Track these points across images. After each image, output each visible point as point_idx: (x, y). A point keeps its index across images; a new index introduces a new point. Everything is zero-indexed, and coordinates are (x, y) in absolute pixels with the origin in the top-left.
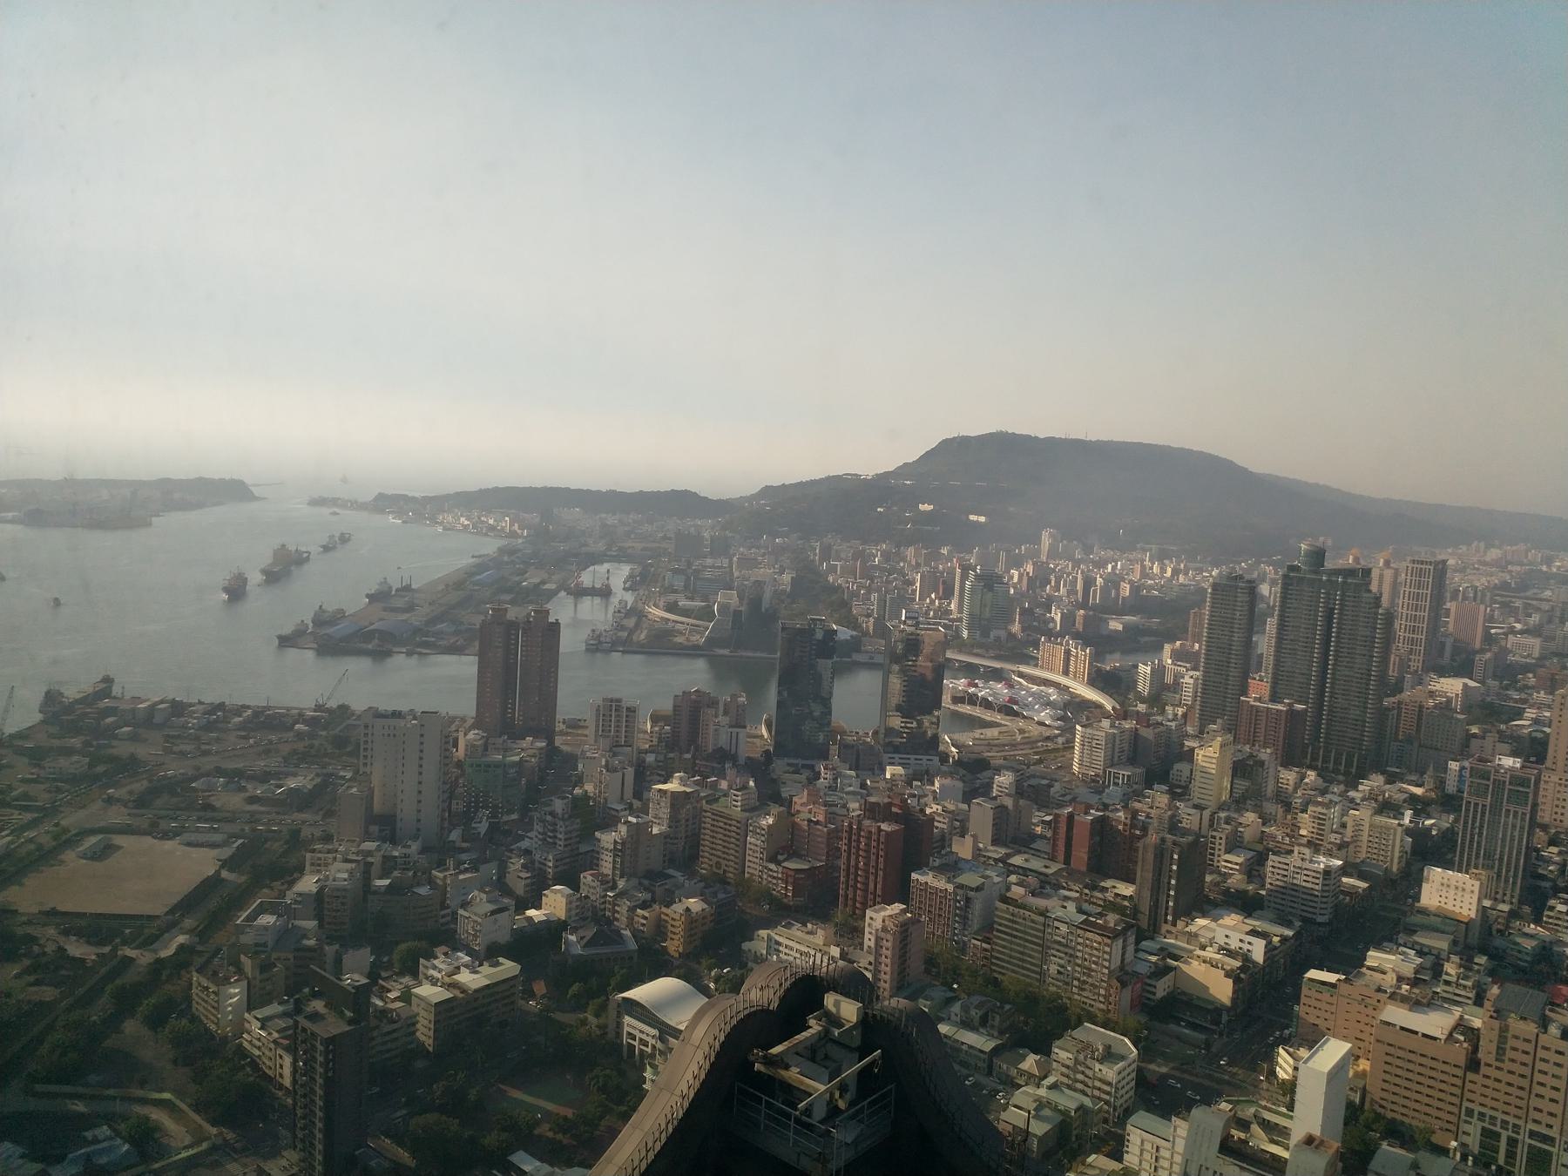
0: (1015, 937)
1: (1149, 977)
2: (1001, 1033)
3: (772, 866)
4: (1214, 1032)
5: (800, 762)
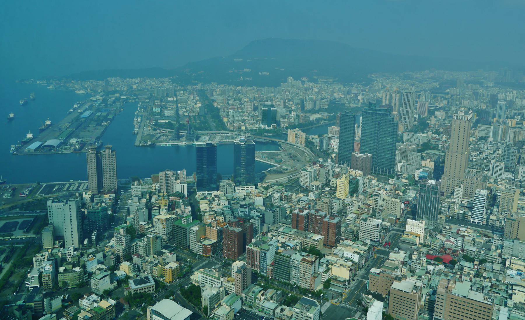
0: (281, 265)
1: (323, 273)
2: (277, 302)
3: (199, 244)
4: (344, 288)
5: (206, 192)
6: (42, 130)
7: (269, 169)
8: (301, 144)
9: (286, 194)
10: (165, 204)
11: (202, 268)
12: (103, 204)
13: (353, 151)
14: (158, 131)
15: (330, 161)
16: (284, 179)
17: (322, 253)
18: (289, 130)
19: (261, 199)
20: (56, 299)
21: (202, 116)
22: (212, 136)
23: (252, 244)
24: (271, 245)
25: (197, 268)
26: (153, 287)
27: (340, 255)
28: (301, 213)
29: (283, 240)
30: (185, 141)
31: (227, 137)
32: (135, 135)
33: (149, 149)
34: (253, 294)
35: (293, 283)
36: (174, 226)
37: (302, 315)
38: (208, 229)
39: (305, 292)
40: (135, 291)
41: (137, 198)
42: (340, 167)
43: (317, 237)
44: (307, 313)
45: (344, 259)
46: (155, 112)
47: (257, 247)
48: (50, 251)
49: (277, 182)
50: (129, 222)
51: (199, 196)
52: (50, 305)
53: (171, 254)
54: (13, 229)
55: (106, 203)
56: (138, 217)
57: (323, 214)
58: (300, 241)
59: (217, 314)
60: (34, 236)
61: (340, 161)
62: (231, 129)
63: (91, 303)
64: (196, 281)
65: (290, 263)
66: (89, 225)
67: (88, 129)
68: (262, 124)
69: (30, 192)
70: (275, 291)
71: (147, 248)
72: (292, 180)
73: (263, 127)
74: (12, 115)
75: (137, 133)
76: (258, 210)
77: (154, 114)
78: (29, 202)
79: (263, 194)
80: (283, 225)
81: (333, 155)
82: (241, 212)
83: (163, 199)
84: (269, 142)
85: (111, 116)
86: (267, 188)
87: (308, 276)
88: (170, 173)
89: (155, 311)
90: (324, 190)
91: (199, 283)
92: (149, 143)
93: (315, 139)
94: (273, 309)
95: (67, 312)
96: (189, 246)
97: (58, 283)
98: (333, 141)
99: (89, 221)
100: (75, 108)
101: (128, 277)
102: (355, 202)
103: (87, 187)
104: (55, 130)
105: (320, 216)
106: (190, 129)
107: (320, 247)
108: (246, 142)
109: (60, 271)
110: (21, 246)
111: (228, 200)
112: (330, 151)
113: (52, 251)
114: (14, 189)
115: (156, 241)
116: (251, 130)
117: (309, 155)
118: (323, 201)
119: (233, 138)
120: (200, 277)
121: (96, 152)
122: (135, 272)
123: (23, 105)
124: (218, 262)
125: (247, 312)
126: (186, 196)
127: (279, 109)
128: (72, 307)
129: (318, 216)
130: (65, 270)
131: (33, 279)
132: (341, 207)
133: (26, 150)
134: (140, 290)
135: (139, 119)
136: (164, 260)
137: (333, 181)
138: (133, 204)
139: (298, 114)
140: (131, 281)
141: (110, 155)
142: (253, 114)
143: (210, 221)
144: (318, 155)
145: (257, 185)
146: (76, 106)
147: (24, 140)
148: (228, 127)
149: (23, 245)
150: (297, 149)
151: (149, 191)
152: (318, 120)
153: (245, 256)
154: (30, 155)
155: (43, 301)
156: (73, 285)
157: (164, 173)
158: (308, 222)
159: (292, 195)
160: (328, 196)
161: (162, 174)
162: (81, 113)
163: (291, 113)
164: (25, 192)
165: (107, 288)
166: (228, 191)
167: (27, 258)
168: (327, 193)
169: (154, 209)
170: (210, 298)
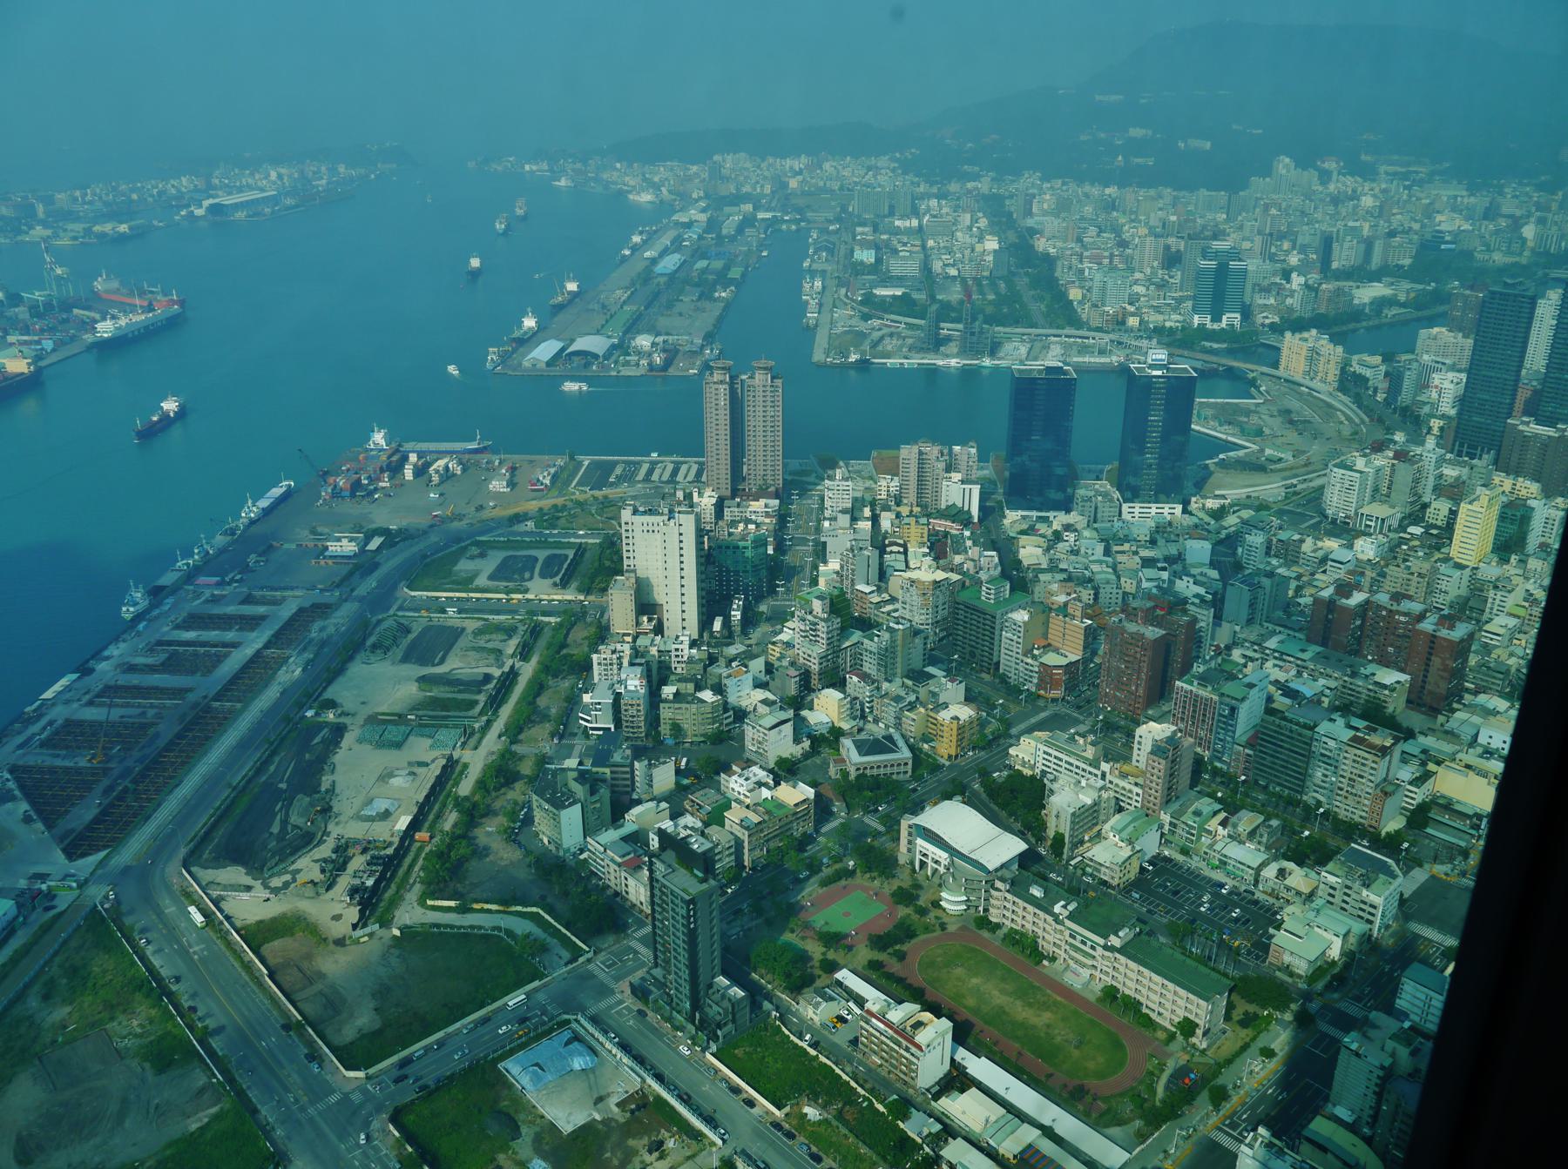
1: (1410, 783)
2: (1268, 848)
3: (1029, 661)
4: (1473, 836)
5: (1034, 514)
6: (560, 308)
7: (1221, 456)
8: (1323, 381)
9: (1283, 535)
10: (920, 540)
11: (1039, 726)
12: (752, 527)
13: (1509, 415)
14: (876, 323)
15: (1431, 442)
16: (1271, 489)
17: (1405, 725)
18: (1288, 334)
19: (1207, 546)
21: (999, 278)
22: (1038, 345)
23: (1194, 677)
24: (1251, 686)
25: (1022, 726)
26: (906, 764)
27: (1466, 737)
28: (1344, 601)
29: (1281, 676)
30: (957, 356)
31: (1083, 350)
32: (811, 331)
33: (852, 373)
34: (1197, 819)
35: (1312, 802)
36: (955, 605)
37: (1345, 894)
38: (1056, 622)
39: (1350, 831)
40: (858, 769)
41: (848, 517)
42: (1459, 464)
43: (1389, 677)
44: (1365, 893)
45: (1480, 750)
46: (862, 263)
47: (1210, 688)
48: (629, 639)
49: (1249, 497)
50: (827, 583)
51: (1015, 522)
53: (952, 681)
54: (527, 575)
55: (758, 525)
56: (853, 570)
57: (1416, 607)
58: (1333, 684)
59: (1091, 860)
60: (582, 598)
61: (1462, 445)
62: (1095, 323)
63: (751, 787)
64: (1024, 764)
65: (1310, 745)
66: (721, 581)
67: (679, 307)
68: (1195, 310)
69: (555, 478)
70: (1262, 818)
71: (886, 658)
72: (1295, 493)
73: (1196, 320)
74: (475, 263)
75: (816, 325)
76: (1199, 578)
77: (859, 269)
78: (555, 506)
79: (1209, 532)
80: (1278, 629)
81: (1436, 424)
82: (1149, 580)
83: (913, 523)
84: (1216, 370)
85: (735, 273)
86: (1219, 514)
87: (1366, 787)
88: (932, 451)
89: (924, 828)
90: (1405, 532)
91: (1033, 767)
92: (853, 358)
93: (1370, 366)
94: (1255, 865)
96: (998, 663)
97: (658, 724)
98: (1436, 379)
99: (720, 571)
100: (636, 244)
101: (836, 733)
102: (1516, 580)
103: (699, 474)
104: (591, 307)
105: (1405, 614)
106: (974, 319)
107: (1395, 705)
108: (1168, 369)
110: (552, 620)
111: (1102, 540)
112: (1426, 409)
114: (513, 469)
115: (913, 642)
116: (1159, 331)
117: (1348, 418)
118: (1408, 568)
119: (1102, 352)
120: (1040, 753)
121: (731, 377)
122: (854, 719)
123: (505, 233)
124: (1082, 718)
125: (1176, 865)
126: (976, 520)
127: (1253, 265)
129: (1398, 612)
130: (677, 694)
132: (1464, 592)
133: (526, 364)
134: (872, 768)
135: (818, 284)
136: (934, 695)
137: (1439, 509)
138: (840, 537)
139: (1310, 282)
140: (847, 743)
141: (769, 388)
142: (1162, 279)
143: (1062, 599)
144: (1380, 421)
145: (1189, 502)
146: (636, 239)
147: (516, 334)
148: (1084, 317)
150: (1310, 399)
151: (868, 497)
152: (1380, 304)
153: (1165, 708)
155: (632, 766)
157: (915, 449)
158: (1361, 627)
159: (1302, 541)
160: (1421, 554)
161: (908, 453)
162: (654, 261)
163: (1288, 281)
165: (786, 755)
166: (1099, 515)
168: (1417, 543)
169: (891, 552)
170: (1073, 814)
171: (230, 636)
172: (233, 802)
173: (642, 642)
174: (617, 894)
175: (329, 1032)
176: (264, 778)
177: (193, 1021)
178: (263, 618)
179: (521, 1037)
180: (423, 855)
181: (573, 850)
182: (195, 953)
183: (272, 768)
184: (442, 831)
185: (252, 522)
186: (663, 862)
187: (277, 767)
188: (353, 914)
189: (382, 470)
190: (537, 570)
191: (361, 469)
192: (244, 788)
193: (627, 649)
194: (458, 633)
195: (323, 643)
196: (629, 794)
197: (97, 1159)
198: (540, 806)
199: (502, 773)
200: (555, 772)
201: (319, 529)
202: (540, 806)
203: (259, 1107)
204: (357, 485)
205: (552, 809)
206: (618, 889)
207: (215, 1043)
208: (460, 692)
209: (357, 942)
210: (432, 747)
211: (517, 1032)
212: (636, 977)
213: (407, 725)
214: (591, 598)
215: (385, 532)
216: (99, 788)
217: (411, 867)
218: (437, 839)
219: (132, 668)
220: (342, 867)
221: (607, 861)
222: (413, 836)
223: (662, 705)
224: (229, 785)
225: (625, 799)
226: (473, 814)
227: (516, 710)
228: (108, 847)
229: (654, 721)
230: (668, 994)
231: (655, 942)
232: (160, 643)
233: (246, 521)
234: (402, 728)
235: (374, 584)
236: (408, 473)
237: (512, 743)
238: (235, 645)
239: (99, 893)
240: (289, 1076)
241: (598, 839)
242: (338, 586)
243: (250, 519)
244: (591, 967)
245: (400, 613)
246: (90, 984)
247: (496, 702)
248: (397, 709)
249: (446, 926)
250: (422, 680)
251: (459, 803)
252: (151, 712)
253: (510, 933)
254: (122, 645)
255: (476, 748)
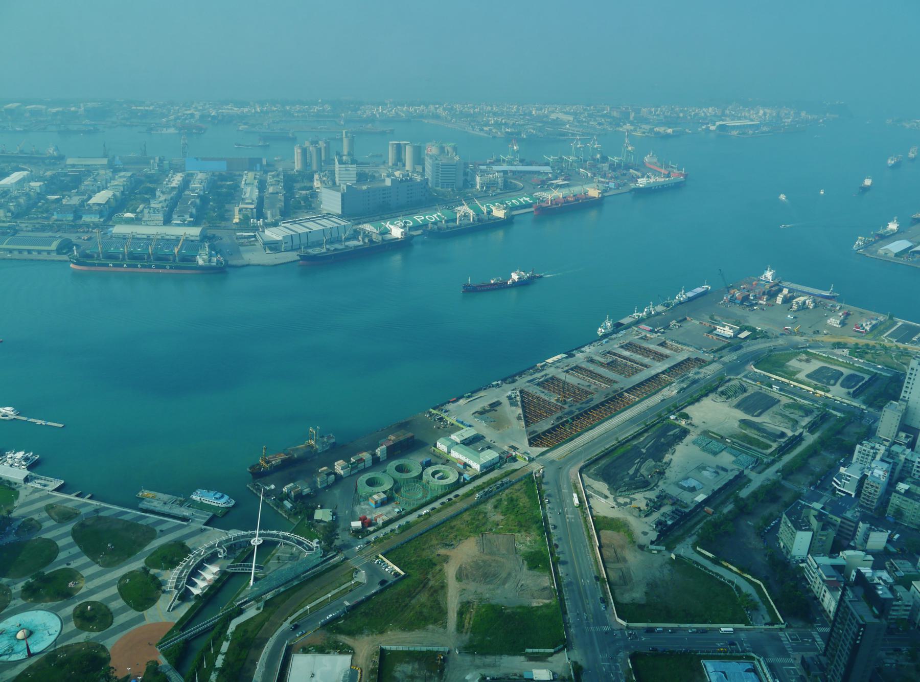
20: (879, 533)
48: (887, 444)
52: (866, 538)
54: (832, 382)
60: (864, 407)
69: (874, 327)
74: (868, 182)
78: (867, 345)
95: (892, 564)
109: (897, 488)
110: (839, 414)
113: (890, 446)
114: (847, 315)
123: (894, 167)
128: (905, 562)
131: (849, 481)
133: (881, 251)
147: (881, 232)
149: (842, 416)
154: (885, 262)
155: (857, 524)
156: (912, 523)
164: (864, 325)
167: (844, 438)
171: (646, 360)
172: (615, 448)
173: (895, 448)
174: (816, 598)
175: (617, 592)
176: (636, 442)
177: (555, 552)
178: (667, 357)
179: (721, 652)
180: (705, 521)
181: (797, 558)
182: (568, 518)
183: (642, 439)
184: (721, 512)
185: (681, 303)
186: (853, 591)
187: (645, 440)
188: (654, 535)
189: (764, 294)
190: (840, 381)
191: (752, 290)
192: (624, 443)
193: (882, 449)
194: (776, 402)
195: (695, 382)
196: (849, 541)
197: (488, 595)
198: (785, 523)
199: (770, 493)
200: (803, 507)
201: (716, 317)
202: (785, 523)
203: (568, 612)
204: (746, 298)
205: (792, 527)
206: (818, 595)
207: (561, 569)
208: (763, 437)
209: (650, 551)
210: (734, 461)
211: (720, 648)
212: (808, 655)
213: (724, 444)
214: (871, 410)
215: (753, 330)
216: (556, 416)
217: (696, 524)
218: (716, 516)
219: (592, 361)
220: (658, 508)
221: (816, 575)
222: (703, 508)
223: (894, 494)
224: (617, 439)
225: (845, 542)
226: (743, 509)
227: (794, 460)
228: (548, 446)
229: (884, 501)
230: (826, 677)
231: (829, 640)
232: (609, 353)
233: (677, 301)
234: (721, 445)
235: (735, 358)
236: (779, 299)
237: (784, 478)
238: (646, 366)
239: (536, 467)
240: (588, 604)
241: (815, 558)
242: (714, 352)
243: (680, 301)
244: (781, 634)
245: (744, 379)
246: (516, 510)
247: (783, 450)
248: (722, 433)
249: (702, 566)
250: (743, 422)
251: (737, 500)
252: (593, 387)
253: (738, 588)
254: (592, 347)
255: (760, 473)
